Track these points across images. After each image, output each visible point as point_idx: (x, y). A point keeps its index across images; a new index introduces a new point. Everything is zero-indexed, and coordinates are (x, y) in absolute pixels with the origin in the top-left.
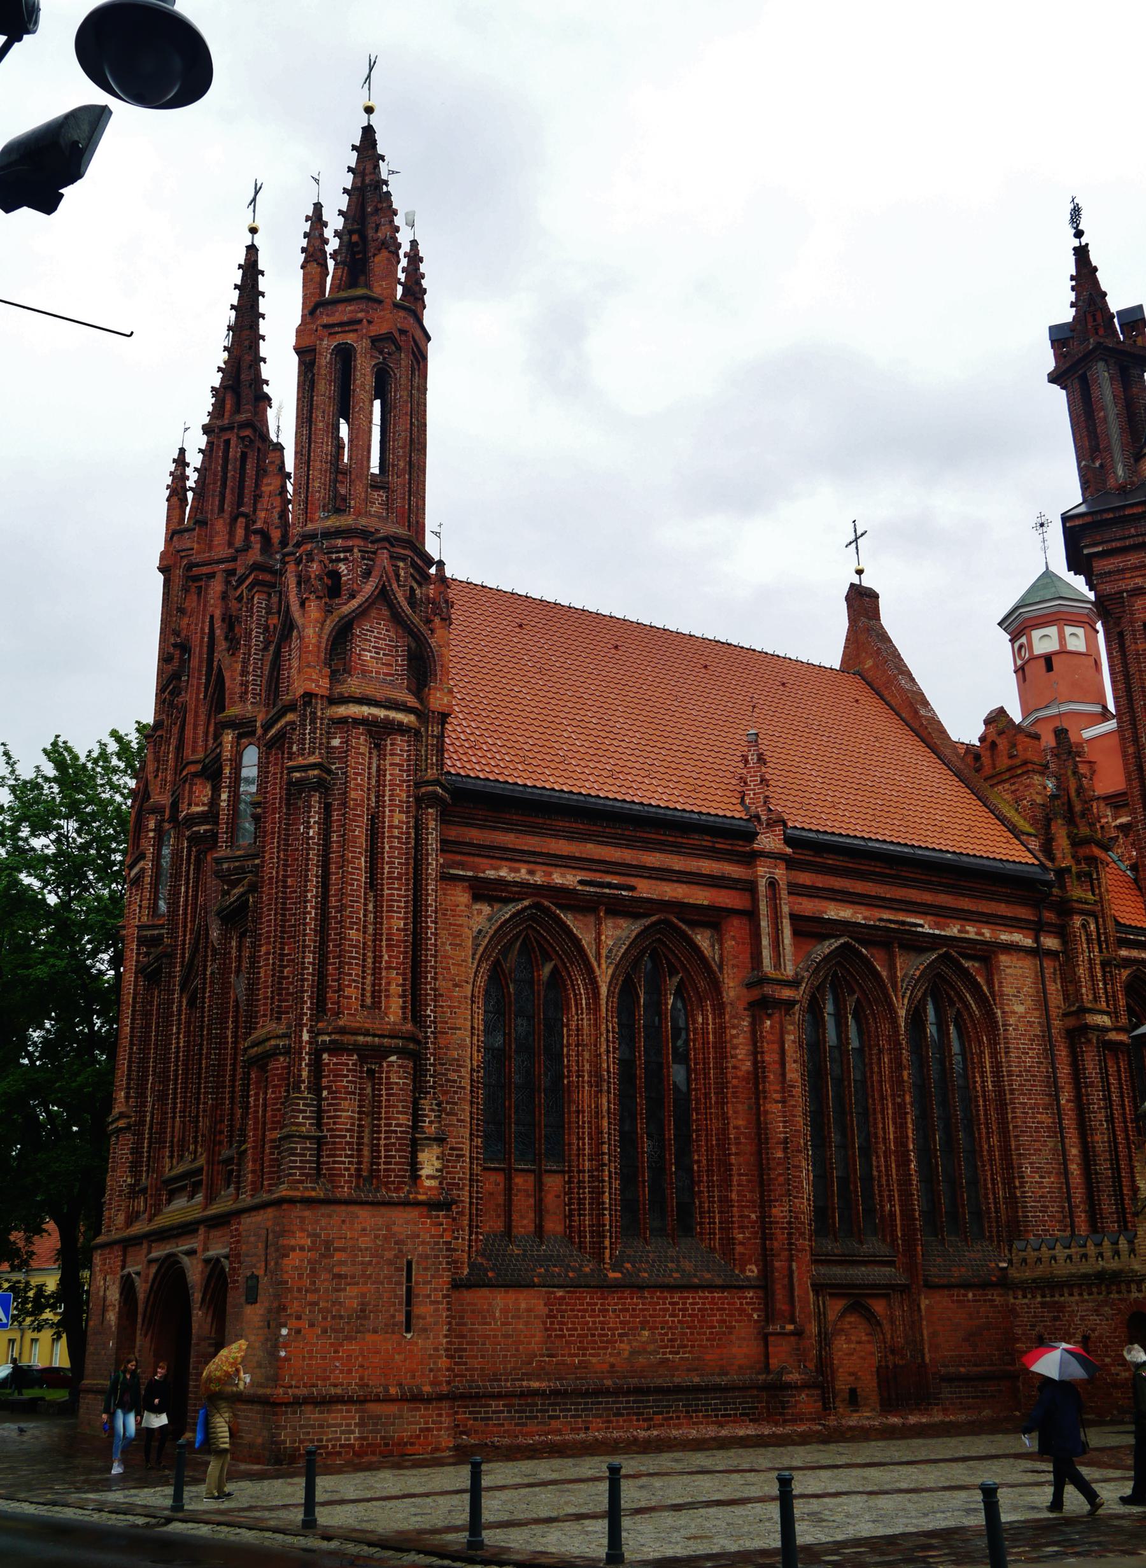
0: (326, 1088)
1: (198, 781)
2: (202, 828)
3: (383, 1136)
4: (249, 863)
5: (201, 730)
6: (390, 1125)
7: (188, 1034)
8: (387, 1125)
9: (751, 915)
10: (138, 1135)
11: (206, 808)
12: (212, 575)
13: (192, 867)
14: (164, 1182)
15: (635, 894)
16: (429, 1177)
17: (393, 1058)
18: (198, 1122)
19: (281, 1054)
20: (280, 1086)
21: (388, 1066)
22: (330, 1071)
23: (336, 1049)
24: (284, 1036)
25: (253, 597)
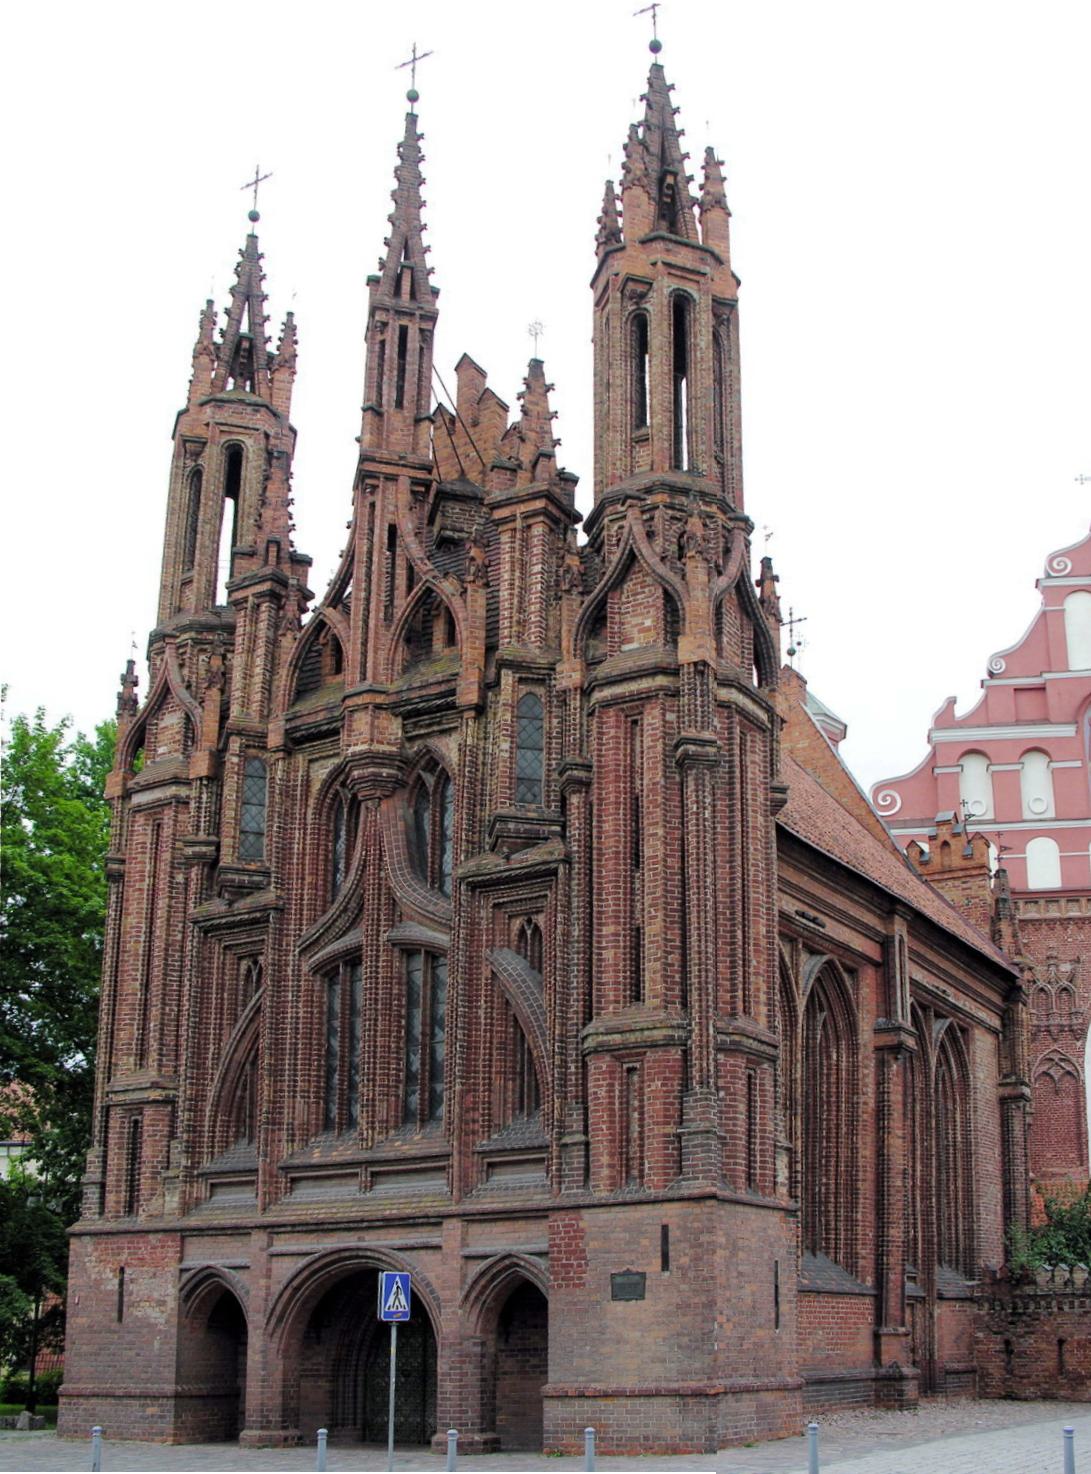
0: (723, 1088)
1: (383, 714)
2: (385, 772)
3: (758, 1141)
4: (546, 828)
5: (382, 655)
6: (764, 1131)
7: (309, 1003)
8: (761, 1131)
9: (884, 965)
10: (195, 1112)
11: (394, 749)
12: (392, 478)
13: (310, 811)
14: (282, 1168)
15: (821, 930)
16: (783, 1184)
17: (765, 1066)
18: (374, 1106)
19: (674, 1045)
20: (673, 1079)
21: (762, 1073)
22: (729, 1071)
23: (732, 1050)
24: (679, 1027)
25: (529, 527)
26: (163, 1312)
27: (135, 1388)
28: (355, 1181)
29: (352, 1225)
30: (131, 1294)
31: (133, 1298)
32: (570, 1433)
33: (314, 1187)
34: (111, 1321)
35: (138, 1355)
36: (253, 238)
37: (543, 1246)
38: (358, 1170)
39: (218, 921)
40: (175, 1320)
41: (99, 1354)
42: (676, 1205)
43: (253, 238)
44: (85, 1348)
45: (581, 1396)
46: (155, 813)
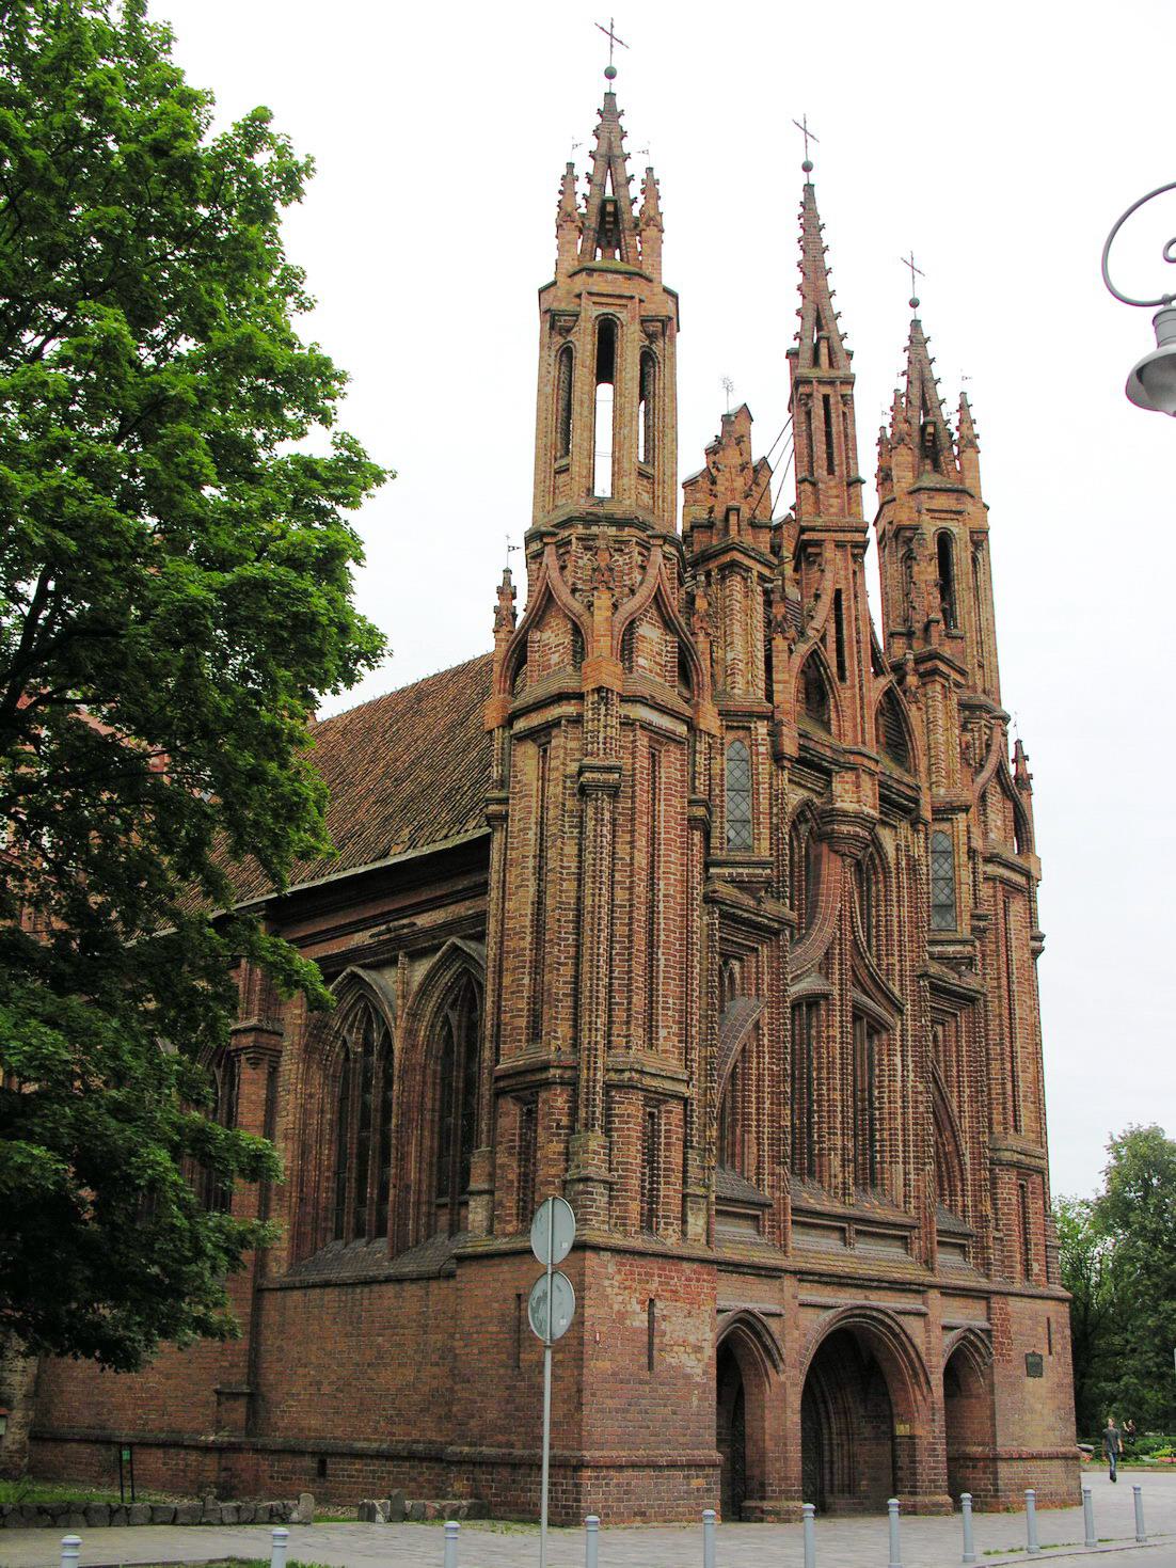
26: (699, 1360)
27: (682, 1456)
28: (836, 1235)
29: (866, 1283)
30: (664, 1334)
31: (666, 1340)
32: (1013, 1491)
33: (803, 1234)
34: (641, 1368)
35: (674, 1413)
36: (610, 97)
37: (986, 1325)
38: (846, 1225)
39: (740, 913)
40: (713, 1371)
41: (628, 1411)
42: (1053, 1303)
43: (610, 97)
44: (608, 1401)
45: (1020, 1458)
46: (658, 741)
